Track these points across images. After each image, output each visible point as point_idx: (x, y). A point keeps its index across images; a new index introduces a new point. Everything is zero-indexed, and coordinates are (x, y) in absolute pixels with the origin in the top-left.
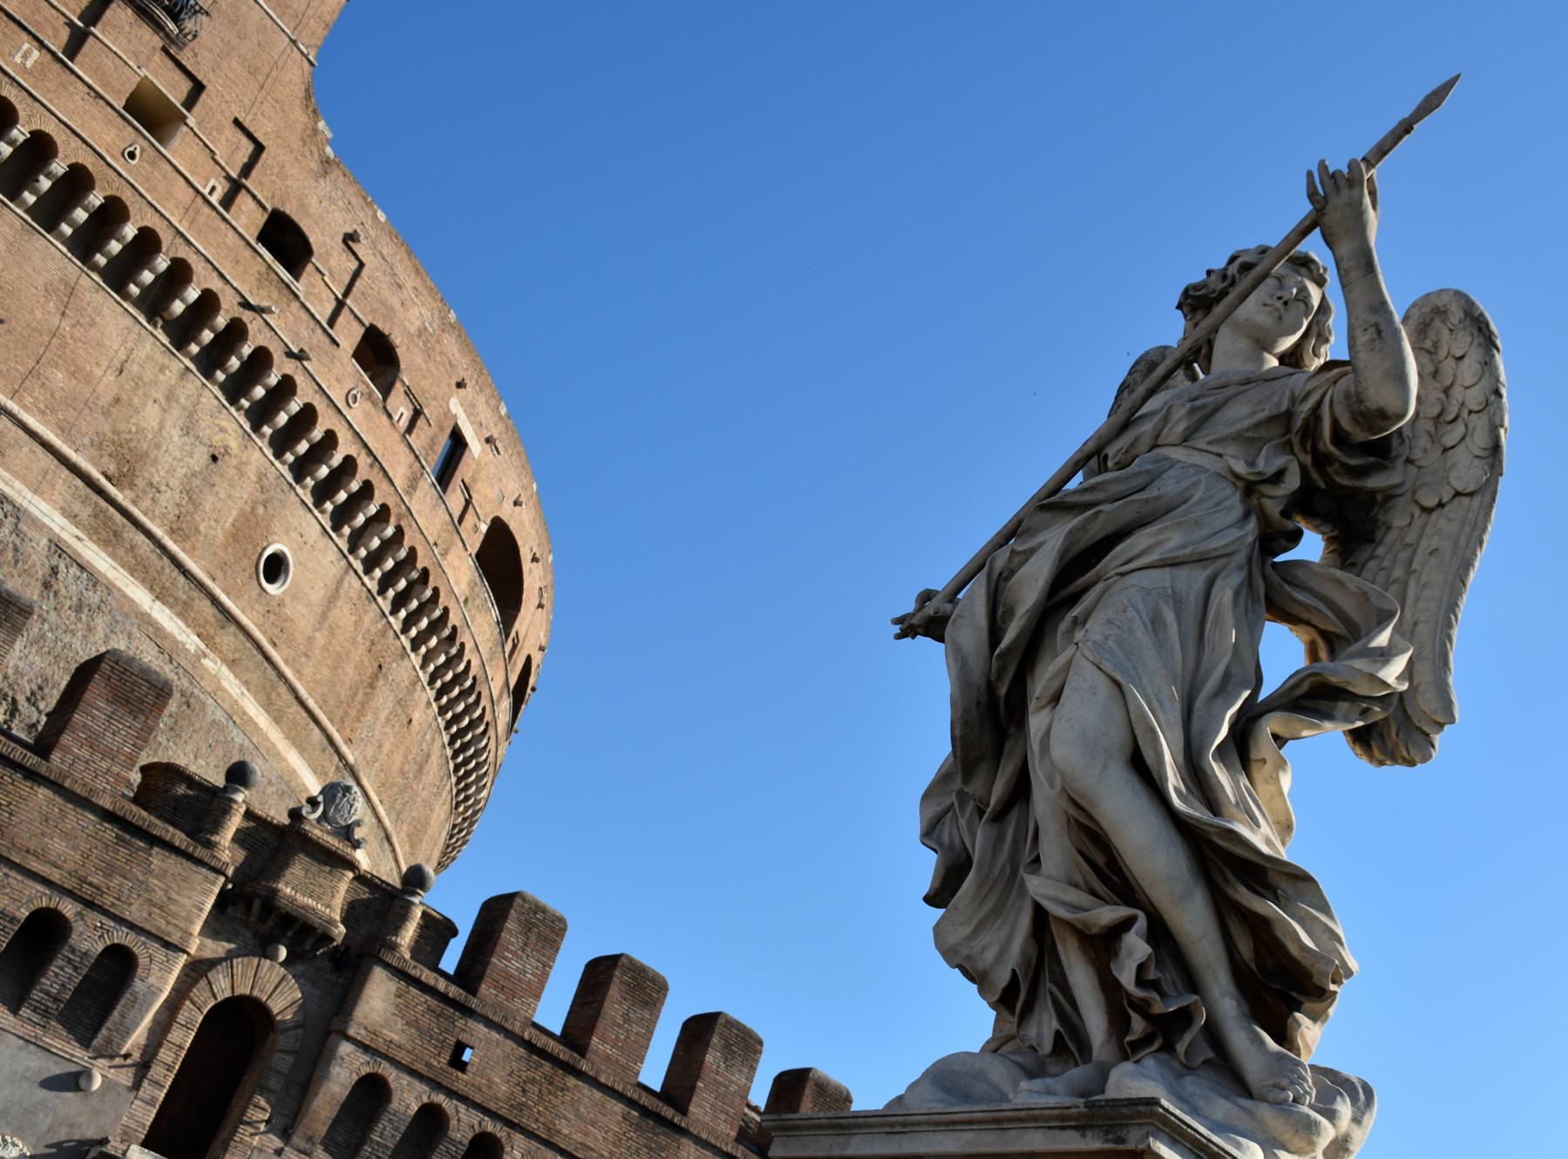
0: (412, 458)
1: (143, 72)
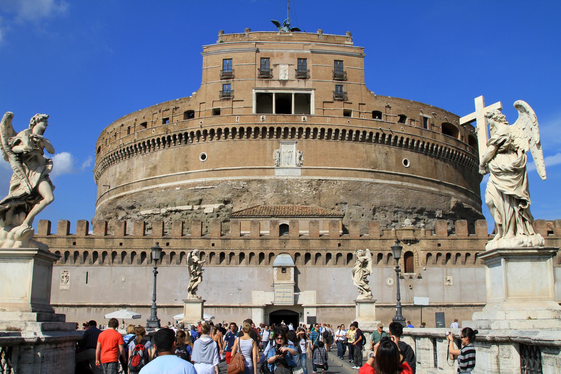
0: (418, 129)
1: (343, 109)
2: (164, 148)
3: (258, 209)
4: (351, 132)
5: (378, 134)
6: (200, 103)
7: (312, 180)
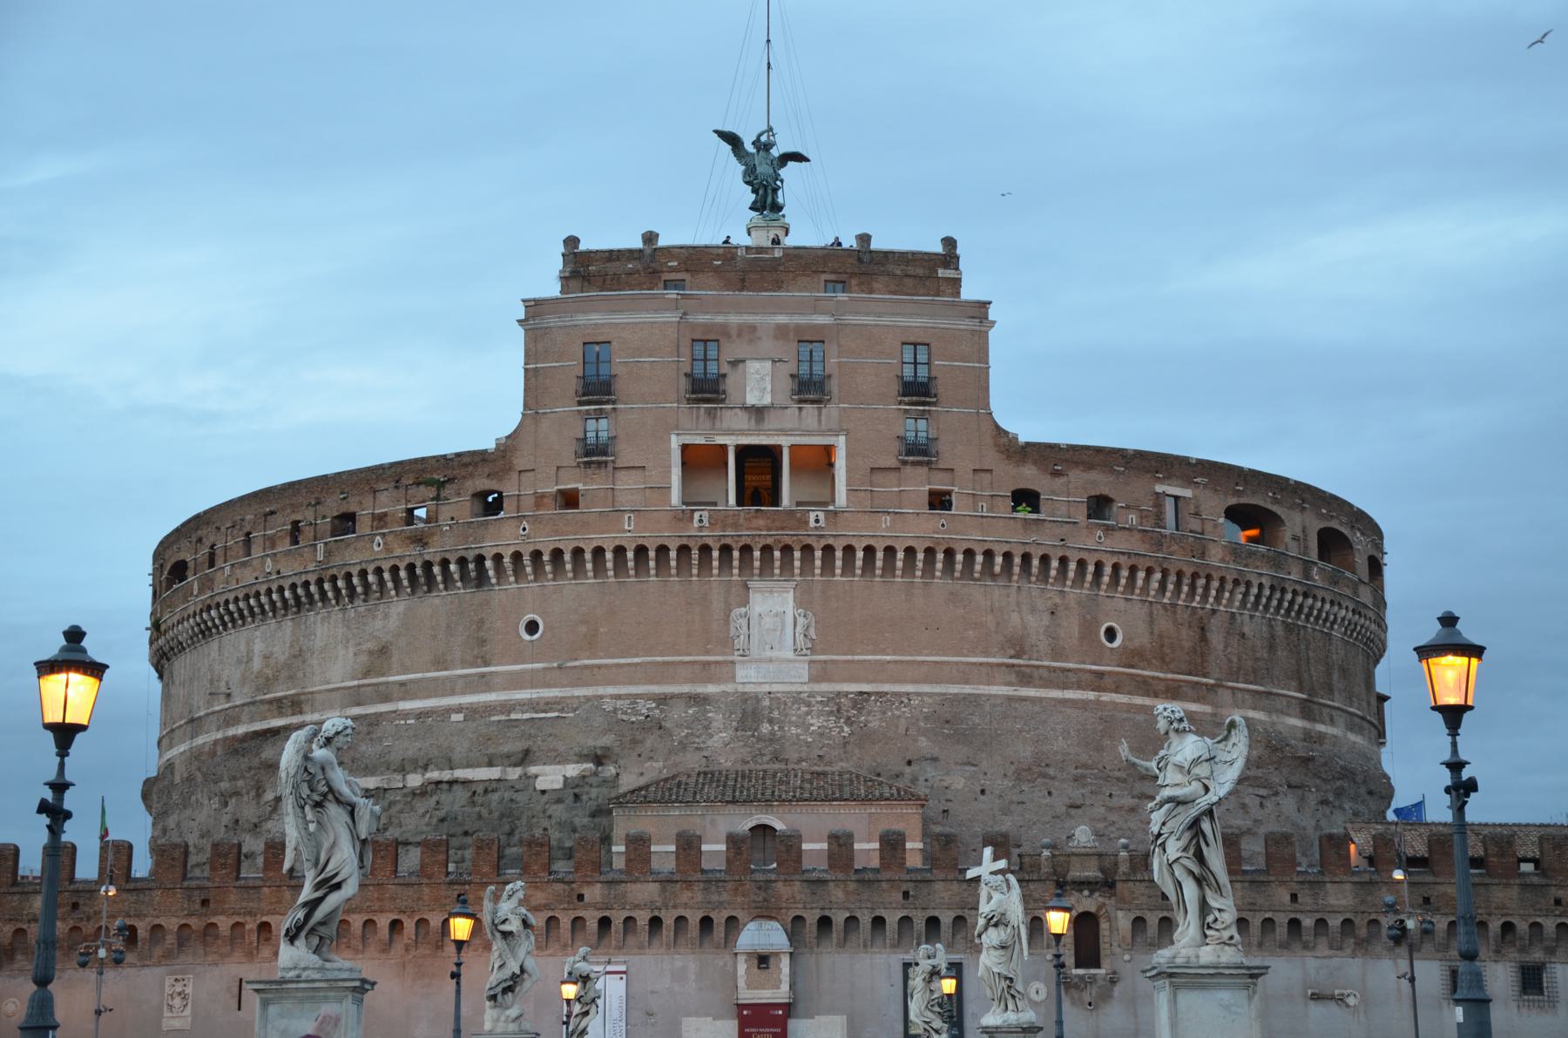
1: (927, 488)
2: (413, 592)
3: (693, 780)
4: (949, 553)
5: (1026, 558)
6: (520, 472)
7: (839, 693)
